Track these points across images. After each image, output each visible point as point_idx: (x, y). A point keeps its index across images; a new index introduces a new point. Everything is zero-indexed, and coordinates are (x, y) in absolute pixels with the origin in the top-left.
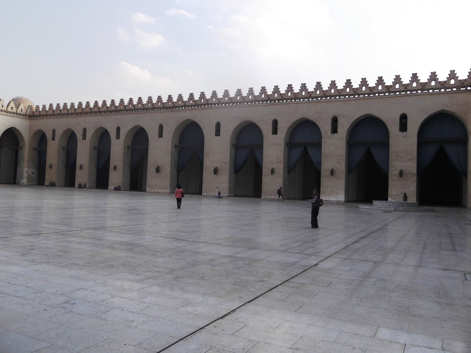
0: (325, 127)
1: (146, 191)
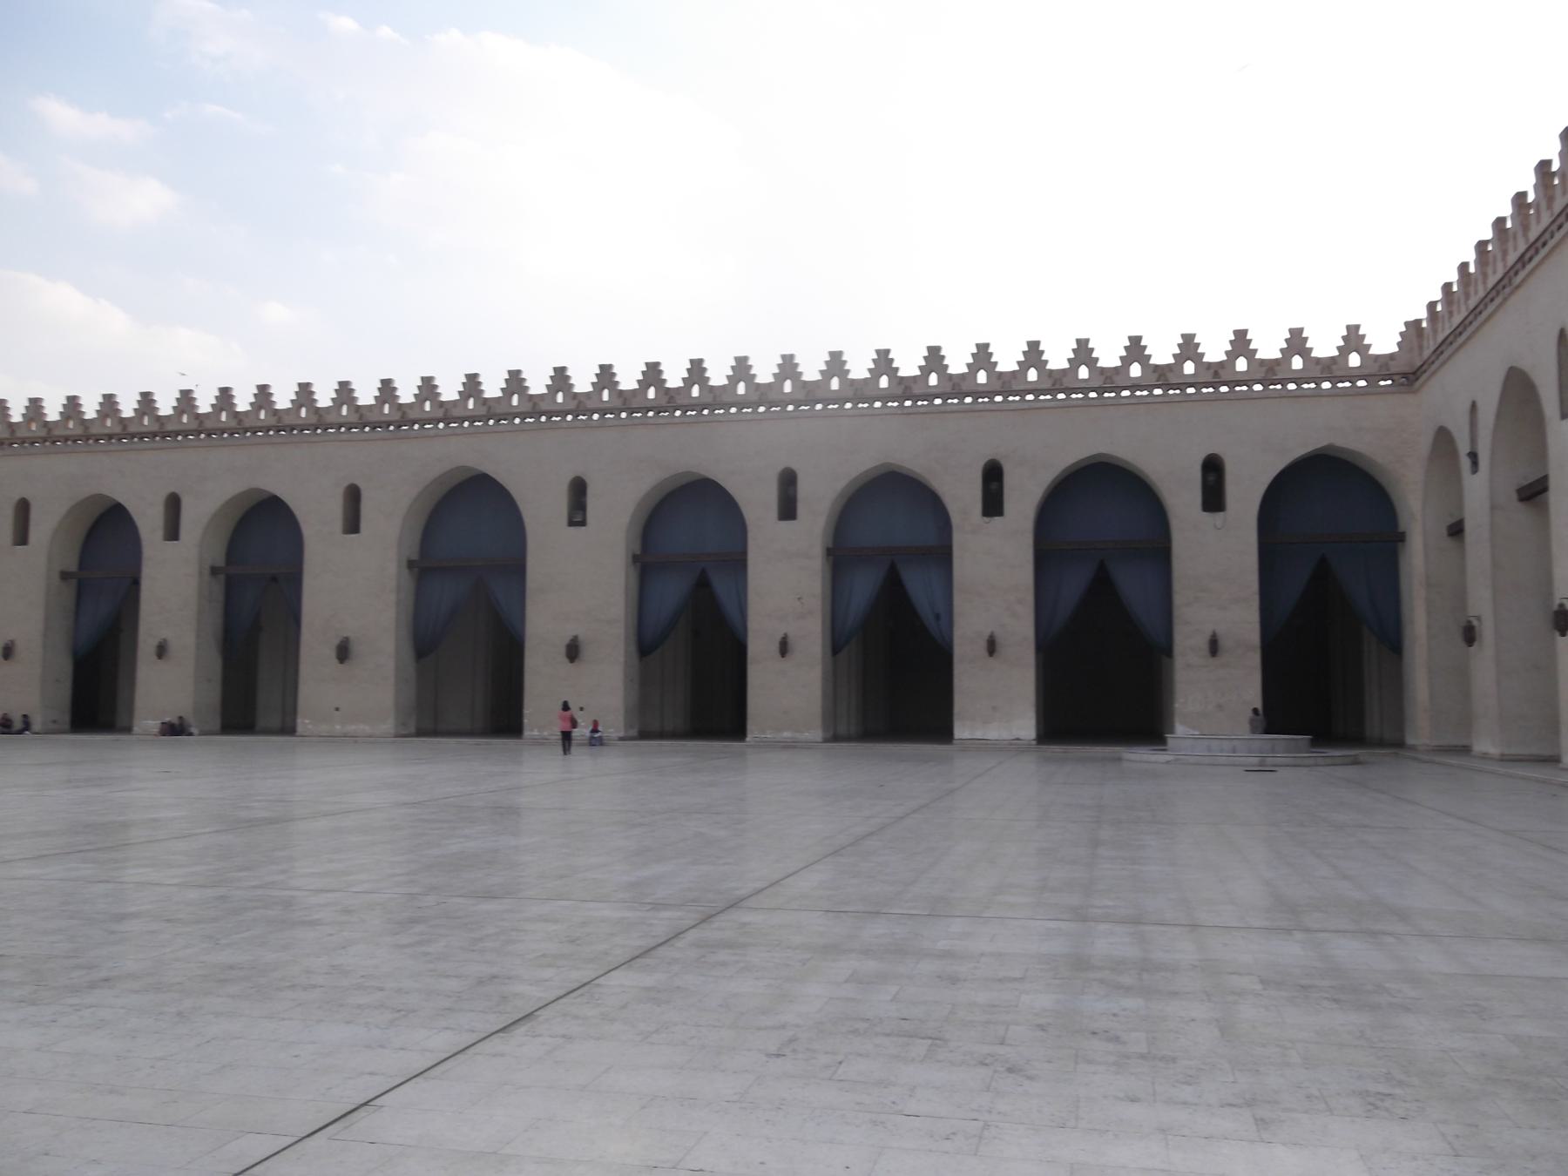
0: (962, 497)
1: (298, 734)
